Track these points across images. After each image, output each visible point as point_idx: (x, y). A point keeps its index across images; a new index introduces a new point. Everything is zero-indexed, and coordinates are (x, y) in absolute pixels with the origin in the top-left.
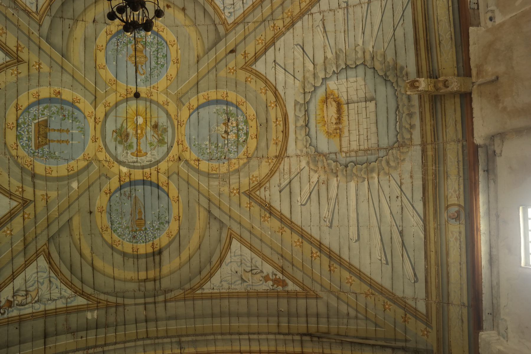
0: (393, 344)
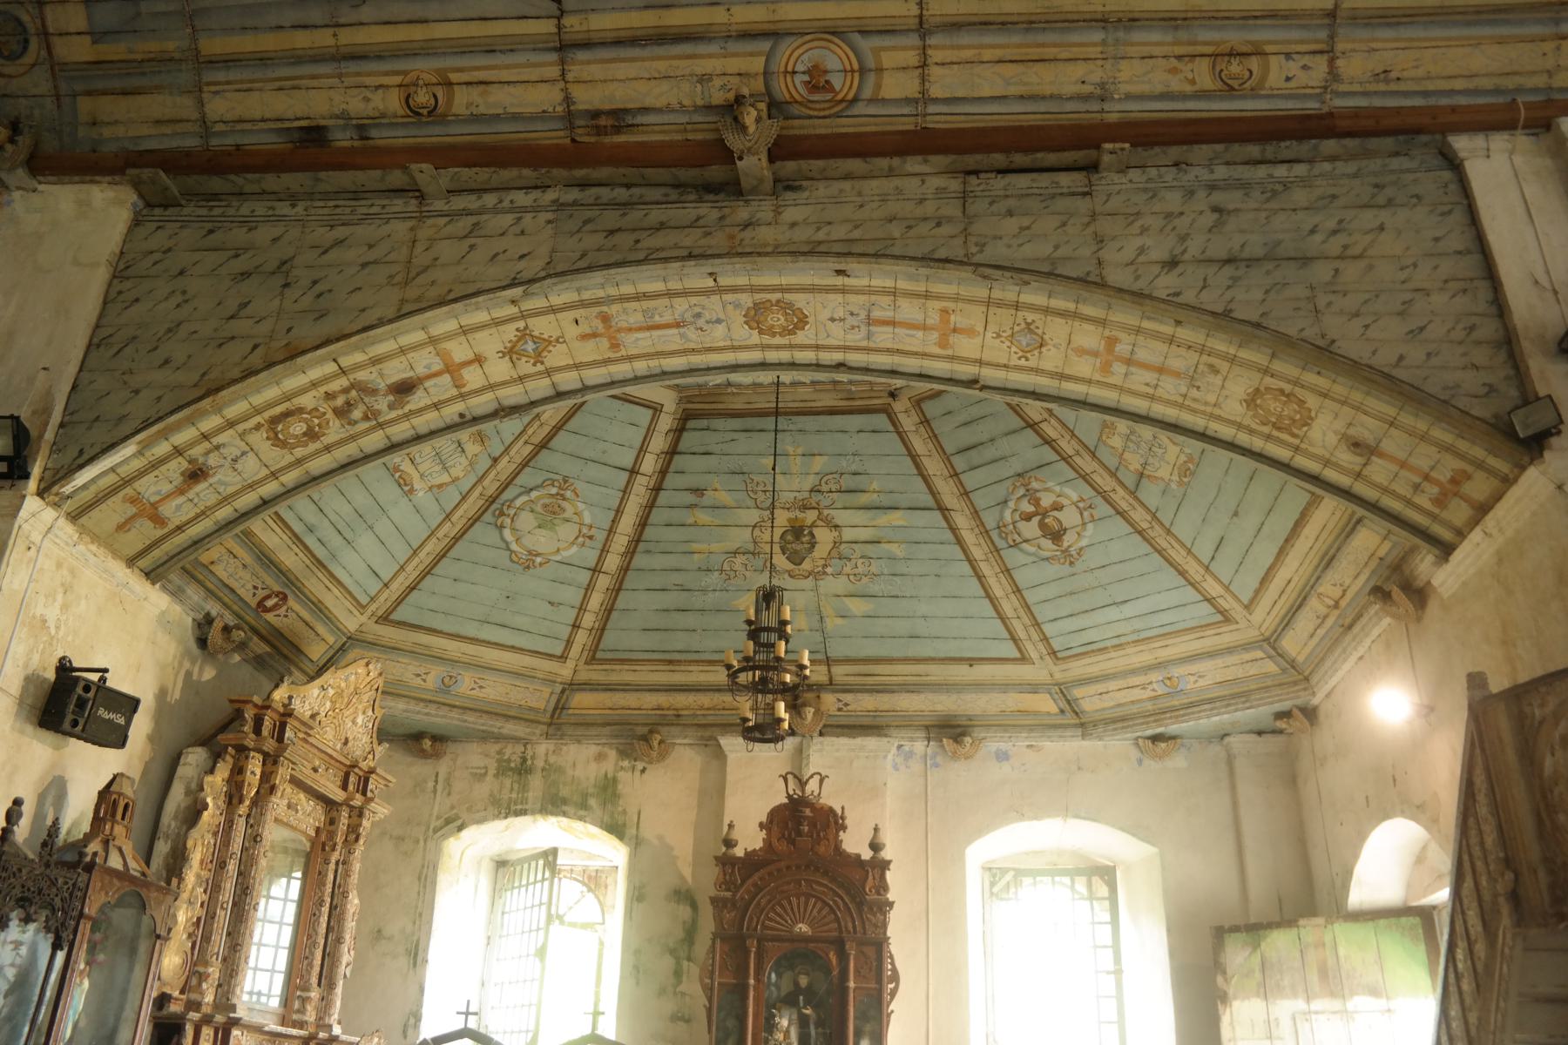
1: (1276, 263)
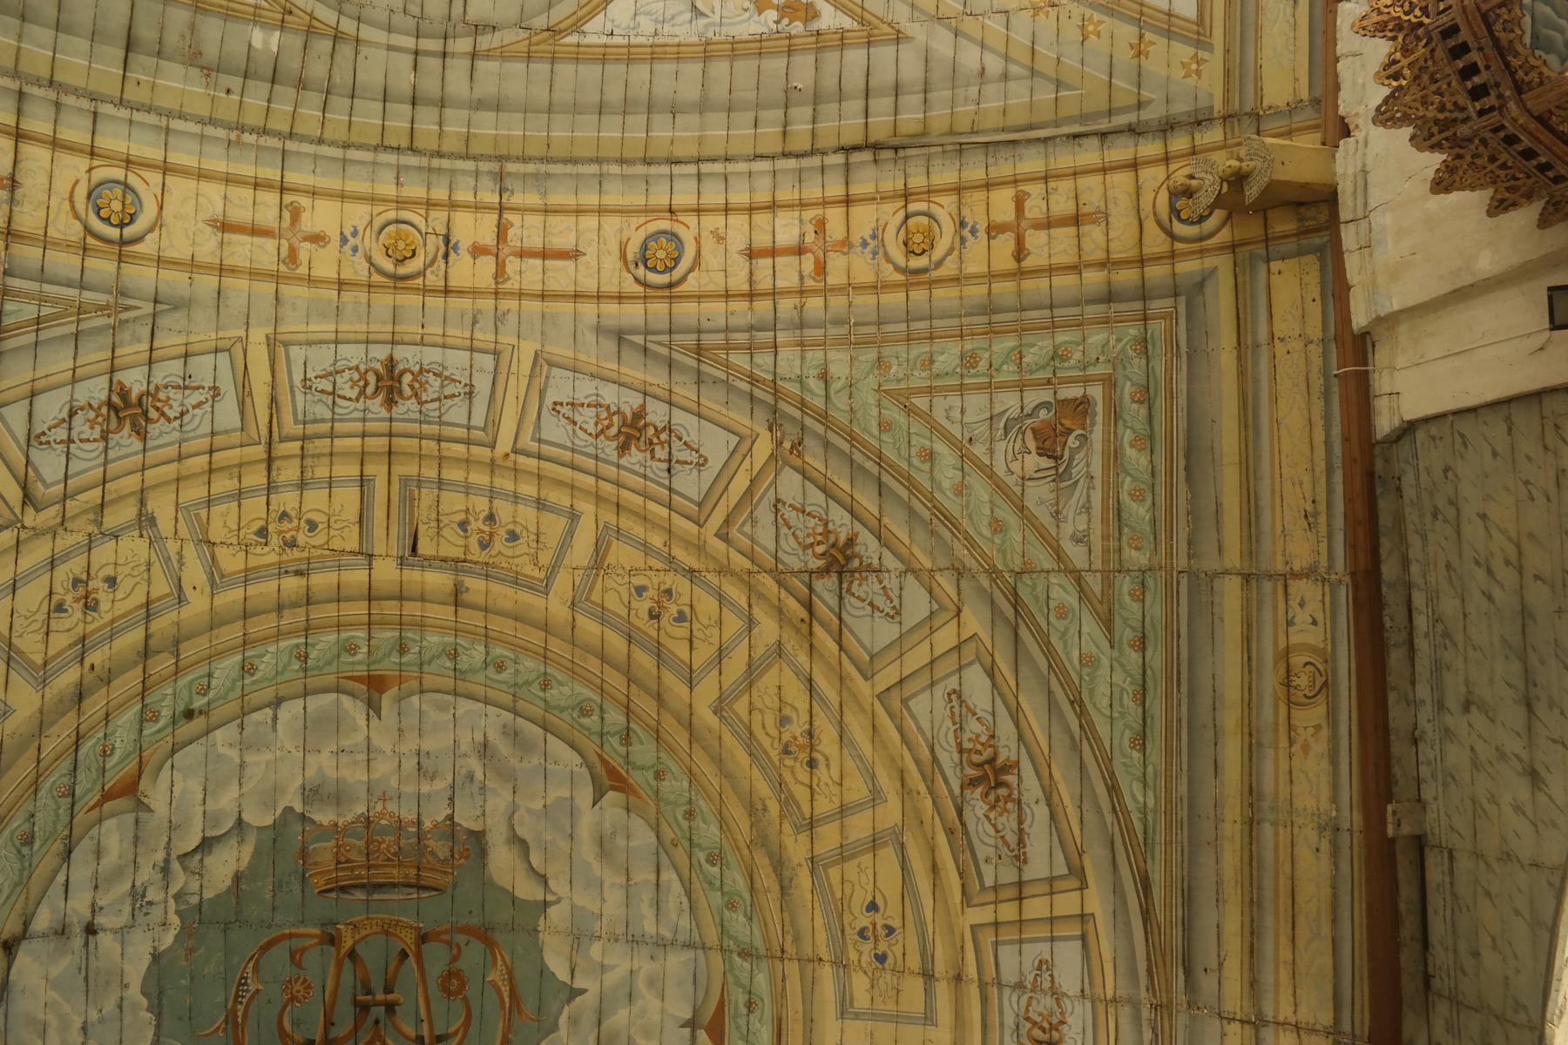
0: (1103, 125)
1: (1529, 650)
